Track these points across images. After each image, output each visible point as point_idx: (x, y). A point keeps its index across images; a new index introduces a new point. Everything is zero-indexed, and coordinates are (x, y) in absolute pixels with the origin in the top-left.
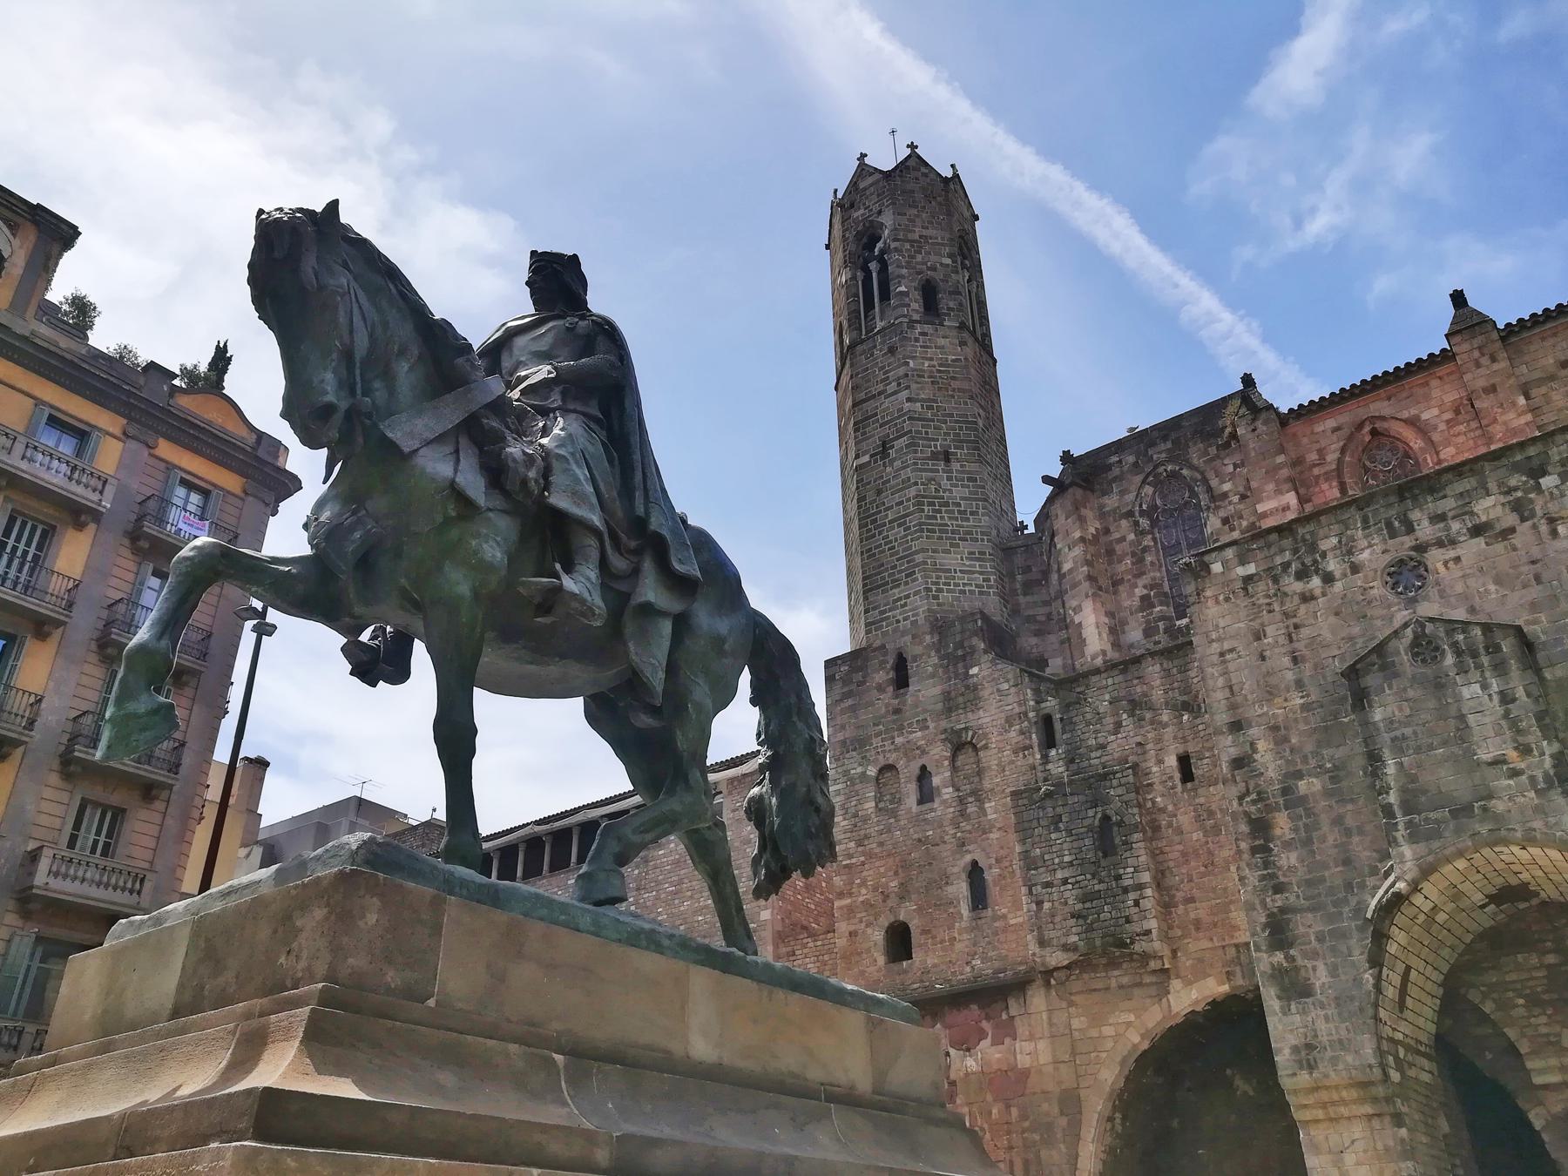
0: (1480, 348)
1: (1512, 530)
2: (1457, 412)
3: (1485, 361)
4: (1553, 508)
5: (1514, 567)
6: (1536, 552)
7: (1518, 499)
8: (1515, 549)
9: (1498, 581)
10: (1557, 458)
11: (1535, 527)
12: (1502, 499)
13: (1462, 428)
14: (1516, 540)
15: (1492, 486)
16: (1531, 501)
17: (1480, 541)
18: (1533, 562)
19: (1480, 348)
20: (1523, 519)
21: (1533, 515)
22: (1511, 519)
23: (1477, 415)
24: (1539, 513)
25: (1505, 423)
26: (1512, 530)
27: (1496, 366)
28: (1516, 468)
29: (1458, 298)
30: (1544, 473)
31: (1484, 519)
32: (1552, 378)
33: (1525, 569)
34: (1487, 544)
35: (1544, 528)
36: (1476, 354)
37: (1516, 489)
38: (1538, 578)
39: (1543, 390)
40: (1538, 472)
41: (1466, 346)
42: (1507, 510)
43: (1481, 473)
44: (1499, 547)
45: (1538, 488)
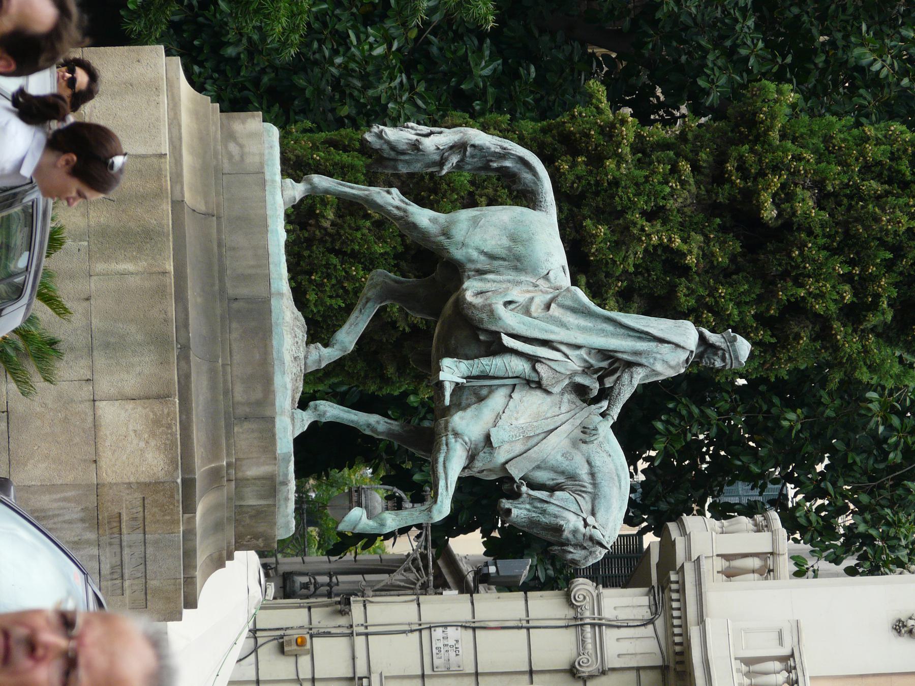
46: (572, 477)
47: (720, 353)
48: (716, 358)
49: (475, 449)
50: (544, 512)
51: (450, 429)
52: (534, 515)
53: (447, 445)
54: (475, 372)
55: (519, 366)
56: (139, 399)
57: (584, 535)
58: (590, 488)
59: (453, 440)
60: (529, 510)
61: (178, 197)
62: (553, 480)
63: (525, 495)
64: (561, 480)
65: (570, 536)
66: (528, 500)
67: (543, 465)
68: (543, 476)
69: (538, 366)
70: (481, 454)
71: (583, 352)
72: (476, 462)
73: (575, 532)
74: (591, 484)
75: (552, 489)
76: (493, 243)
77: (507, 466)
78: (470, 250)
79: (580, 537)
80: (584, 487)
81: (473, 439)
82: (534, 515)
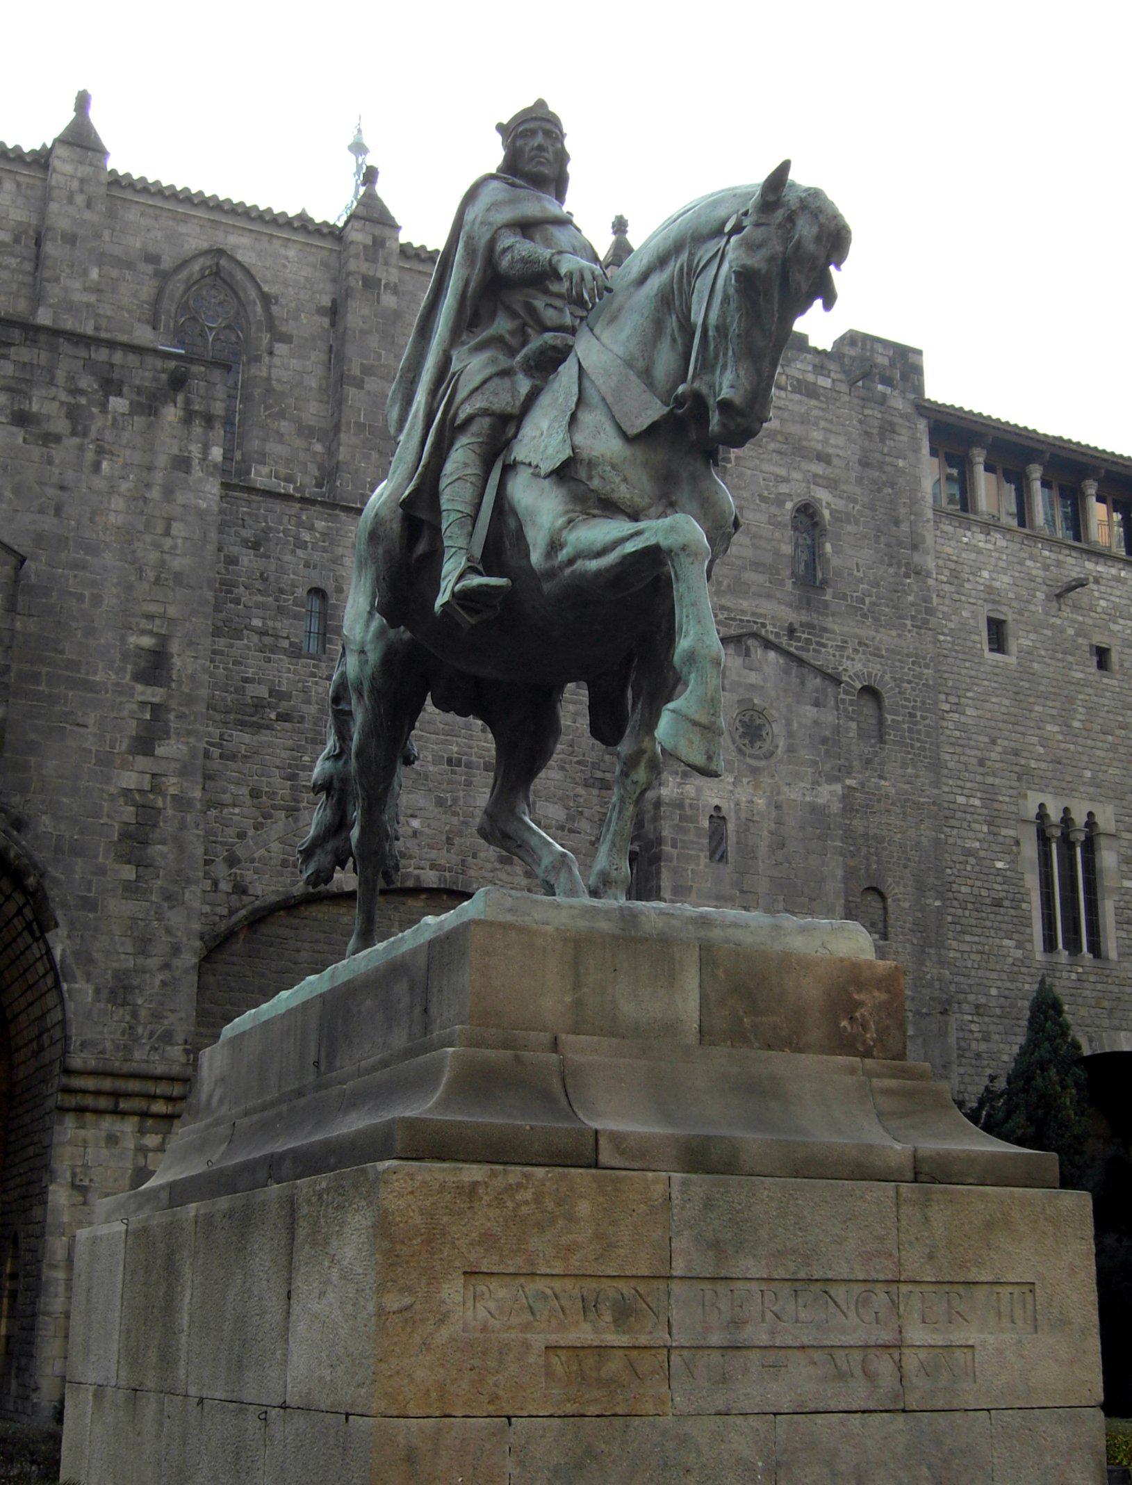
0: (82, 181)
1: (57, 439)
2: (17, 240)
3: (80, 199)
4: (109, 436)
5: (41, 483)
6: (70, 476)
7: (78, 406)
8: (50, 462)
9: (16, 490)
10: (137, 382)
11: (81, 448)
12: (63, 396)
13: (13, 262)
14: (57, 453)
15: (61, 376)
16: (92, 416)
17: (19, 435)
18: (62, 488)
19: (82, 181)
20: (74, 433)
21: (85, 434)
22: (60, 425)
23: (38, 260)
24: (93, 434)
25: (66, 289)
26: (57, 439)
27: (88, 215)
28: (89, 365)
29: (83, 102)
30: (119, 394)
31: (35, 408)
32: (130, 265)
33: (51, 492)
34: (25, 440)
35: (90, 456)
36: (75, 185)
37: (82, 392)
38: (58, 510)
39: (115, 273)
40: (110, 386)
41: (68, 168)
42: (62, 414)
43: (54, 349)
44: (36, 452)
45: (104, 407)
47: (519, 143)
48: (527, 149)
50: (722, 329)
51: (548, 565)
52: (730, 353)
53: (571, 562)
54: (461, 542)
55: (461, 458)
56: (289, 1280)
57: (757, 225)
58: (684, 257)
59: (564, 551)
60: (724, 367)
61: (164, 1195)
62: (674, 340)
63: (696, 385)
64: (672, 323)
65: (763, 253)
67: (640, 364)
68: (665, 360)
69: (458, 421)
71: (455, 355)
72: (616, 496)
73: (751, 246)
74: (677, 257)
75: (687, 328)
76: (361, 600)
77: (632, 431)
78: (370, 636)
79: (760, 233)
80: (681, 269)
81: (561, 508)
82: (730, 353)
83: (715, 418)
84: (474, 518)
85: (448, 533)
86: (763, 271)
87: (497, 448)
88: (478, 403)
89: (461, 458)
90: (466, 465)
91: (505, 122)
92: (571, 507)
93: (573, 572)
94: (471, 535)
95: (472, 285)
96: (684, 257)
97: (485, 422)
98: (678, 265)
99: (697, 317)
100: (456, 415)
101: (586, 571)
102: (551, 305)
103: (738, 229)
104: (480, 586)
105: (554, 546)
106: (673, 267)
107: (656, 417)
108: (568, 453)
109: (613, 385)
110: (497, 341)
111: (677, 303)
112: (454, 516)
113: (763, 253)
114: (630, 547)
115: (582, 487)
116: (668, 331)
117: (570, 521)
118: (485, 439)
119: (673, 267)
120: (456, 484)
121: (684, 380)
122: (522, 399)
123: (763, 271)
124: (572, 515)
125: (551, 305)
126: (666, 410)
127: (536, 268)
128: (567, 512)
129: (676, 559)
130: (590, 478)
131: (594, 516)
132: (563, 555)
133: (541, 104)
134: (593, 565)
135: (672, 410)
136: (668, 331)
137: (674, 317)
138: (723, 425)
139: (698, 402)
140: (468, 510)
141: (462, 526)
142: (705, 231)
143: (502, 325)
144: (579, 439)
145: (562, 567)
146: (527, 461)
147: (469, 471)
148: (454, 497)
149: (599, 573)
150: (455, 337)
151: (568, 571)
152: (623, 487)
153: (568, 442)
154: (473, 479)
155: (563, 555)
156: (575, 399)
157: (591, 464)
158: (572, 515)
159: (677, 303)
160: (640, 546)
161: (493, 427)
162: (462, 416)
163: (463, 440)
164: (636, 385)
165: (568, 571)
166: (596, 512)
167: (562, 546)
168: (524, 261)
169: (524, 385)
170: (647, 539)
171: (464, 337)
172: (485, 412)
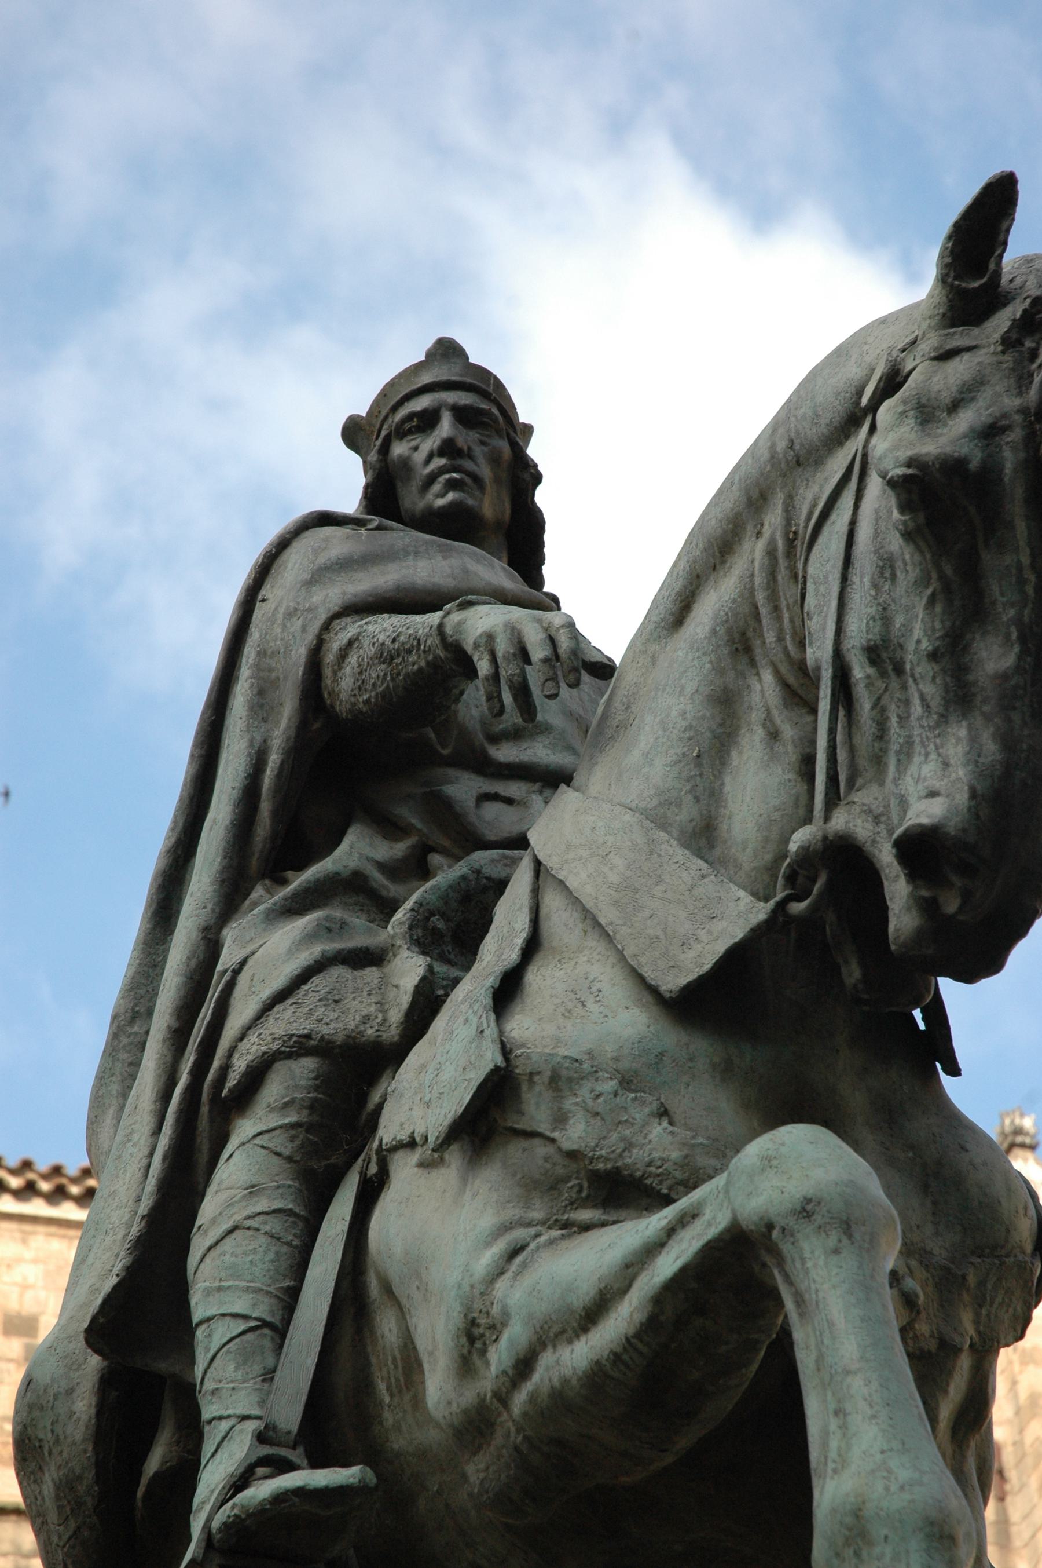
46: (740, 643)
49: (552, 1186)
52: (917, 709)
53: (524, 1366)
54: (244, 1402)
55: (244, 1173)
58: (773, 519)
62: (774, 735)
66: (867, 796)
67: (686, 813)
68: (755, 789)
69: (232, 1080)
70: (576, 1134)
72: (636, 1159)
73: (927, 414)
77: (672, 983)
80: (771, 553)
83: (898, 890)
84: (278, 1330)
85: (209, 1385)
86: (974, 464)
87: (338, 1141)
88: (287, 1021)
89: (244, 1173)
90: (253, 1190)
91: (362, 410)
92: (513, 1212)
93: (533, 1398)
94: (269, 1376)
95: (274, 760)
96: (773, 519)
97: (306, 1067)
98: (761, 545)
99: (819, 653)
100: (225, 1069)
101: (565, 1382)
102: (495, 797)
103: (893, 382)
104: (280, 1498)
105: (474, 1336)
106: (752, 553)
107: (738, 933)
108: (491, 1057)
109: (613, 878)
110: (352, 887)
111: (770, 637)
112: (223, 1331)
113: (966, 420)
114: (667, 1265)
115: (541, 1150)
116: (756, 716)
117: (515, 1252)
118: (304, 1117)
119: (752, 553)
120: (228, 1244)
121: (808, 820)
122: (405, 1000)
123: (974, 464)
124: (520, 1234)
125: (495, 797)
126: (761, 912)
127: (416, 662)
128: (505, 1228)
129: (786, 1248)
130: (561, 1119)
131: (586, 1228)
132: (500, 1356)
133: (447, 350)
134: (578, 1355)
135: (782, 905)
136: (756, 716)
137: (768, 676)
138: (928, 908)
139: (844, 864)
140: (263, 1309)
141: (244, 1358)
142: (813, 433)
143: (356, 850)
144: (521, 1025)
145: (502, 1398)
146: (403, 1136)
147: (263, 1204)
148: (224, 1277)
149: (597, 1377)
150: (231, 898)
151: (520, 1400)
152: (658, 1130)
153: (491, 1031)
154: (273, 1225)
155: (500, 1356)
156: (519, 941)
157: (561, 1079)
158: (520, 1234)
159: (770, 637)
160: (697, 1245)
161: (322, 1082)
162: (240, 1064)
163: (245, 1128)
164: (681, 866)
165: (520, 1400)
166: (585, 1215)
167: (496, 1328)
168: (387, 656)
169: (409, 969)
170: (709, 1224)
171: (258, 892)
172: (300, 1046)
